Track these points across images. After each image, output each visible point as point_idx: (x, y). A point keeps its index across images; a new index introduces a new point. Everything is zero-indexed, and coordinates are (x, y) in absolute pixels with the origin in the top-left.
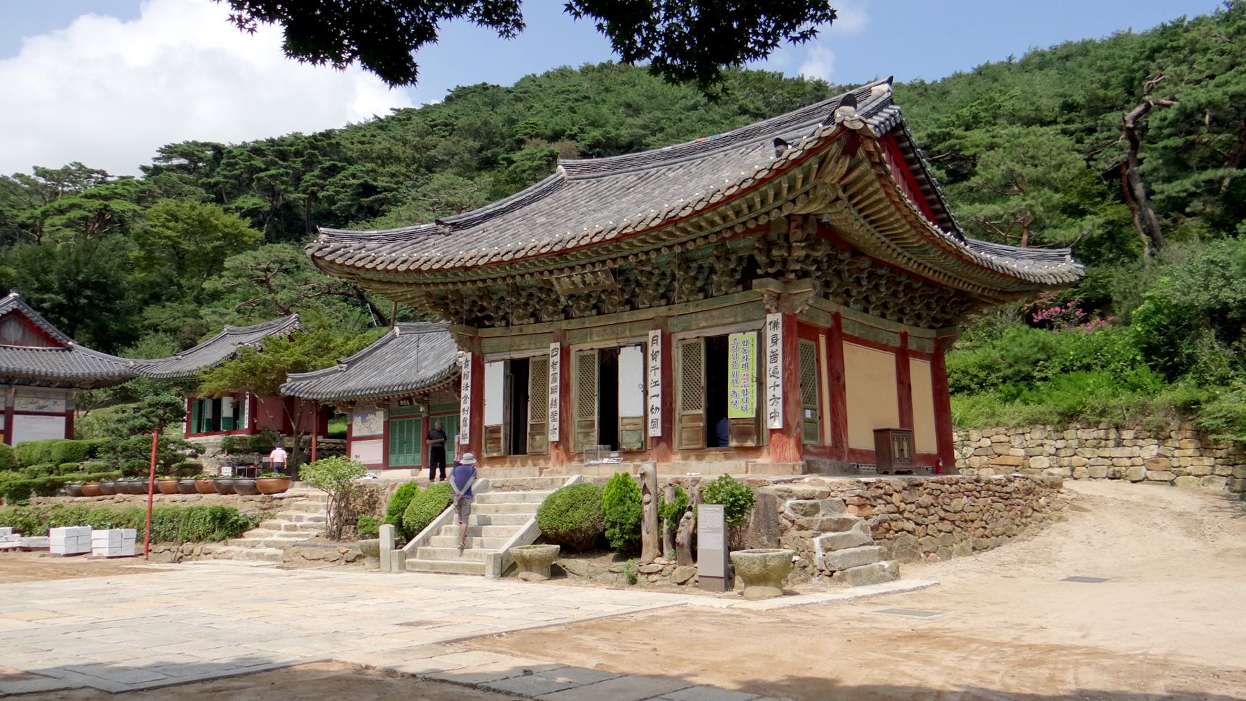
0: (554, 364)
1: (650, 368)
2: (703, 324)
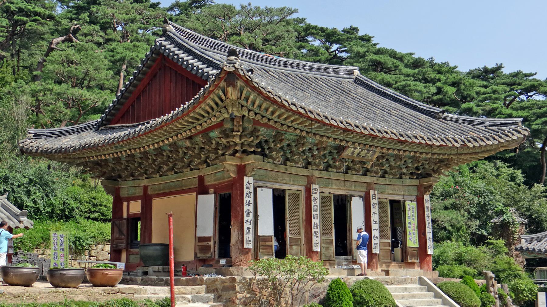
0: (315, 199)
1: (372, 213)
2: (391, 192)
